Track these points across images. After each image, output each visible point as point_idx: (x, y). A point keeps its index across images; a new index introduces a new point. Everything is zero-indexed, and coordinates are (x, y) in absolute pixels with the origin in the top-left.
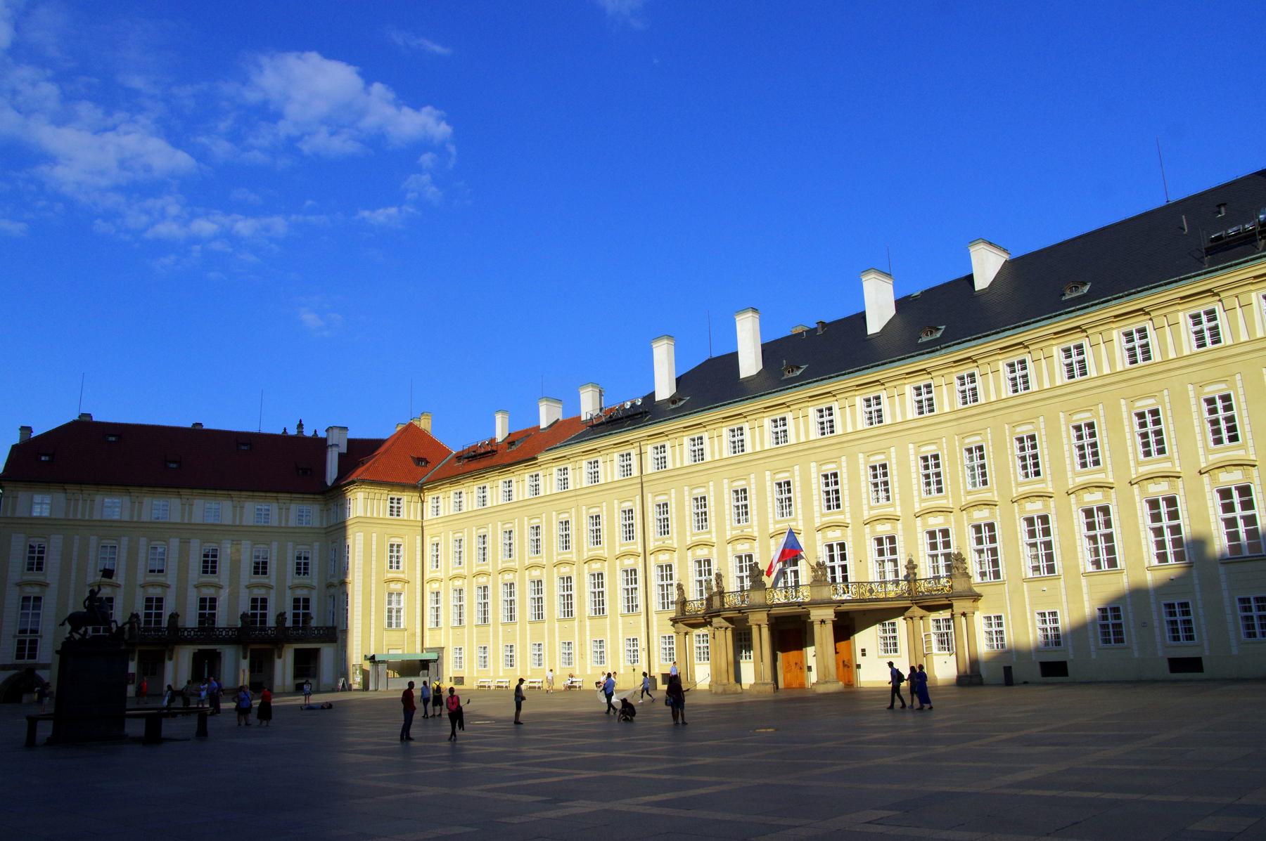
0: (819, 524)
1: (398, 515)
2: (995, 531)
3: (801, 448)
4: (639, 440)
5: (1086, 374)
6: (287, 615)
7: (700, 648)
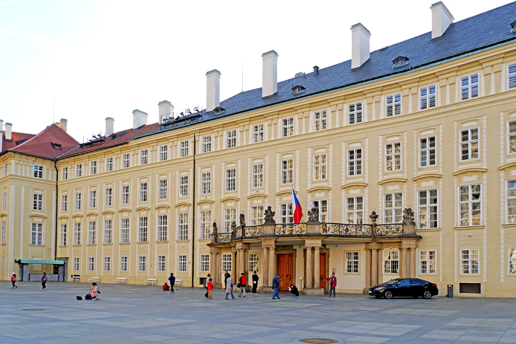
0: (310, 188)
2: (426, 196)
3: (301, 138)
7: (225, 263)
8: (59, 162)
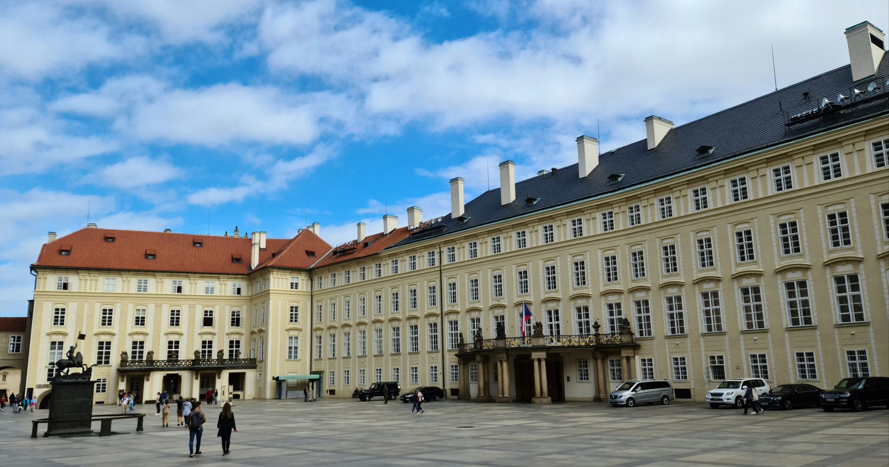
1: (296, 288)
3: (533, 251)
4: (439, 244)
5: (747, 197)
6: (224, 352)
8: (314, 271)
